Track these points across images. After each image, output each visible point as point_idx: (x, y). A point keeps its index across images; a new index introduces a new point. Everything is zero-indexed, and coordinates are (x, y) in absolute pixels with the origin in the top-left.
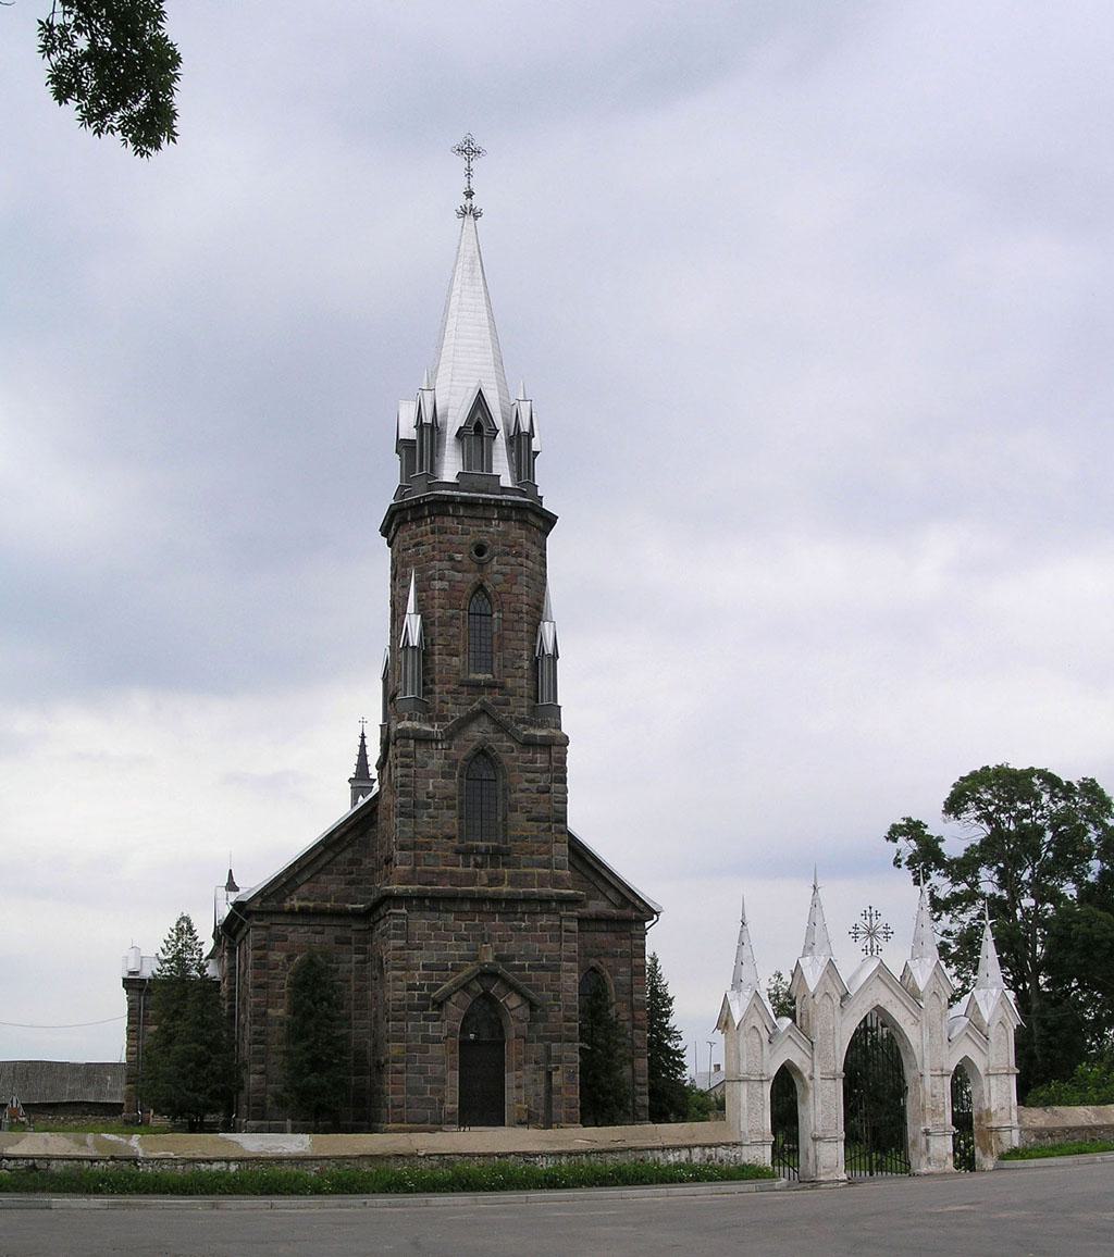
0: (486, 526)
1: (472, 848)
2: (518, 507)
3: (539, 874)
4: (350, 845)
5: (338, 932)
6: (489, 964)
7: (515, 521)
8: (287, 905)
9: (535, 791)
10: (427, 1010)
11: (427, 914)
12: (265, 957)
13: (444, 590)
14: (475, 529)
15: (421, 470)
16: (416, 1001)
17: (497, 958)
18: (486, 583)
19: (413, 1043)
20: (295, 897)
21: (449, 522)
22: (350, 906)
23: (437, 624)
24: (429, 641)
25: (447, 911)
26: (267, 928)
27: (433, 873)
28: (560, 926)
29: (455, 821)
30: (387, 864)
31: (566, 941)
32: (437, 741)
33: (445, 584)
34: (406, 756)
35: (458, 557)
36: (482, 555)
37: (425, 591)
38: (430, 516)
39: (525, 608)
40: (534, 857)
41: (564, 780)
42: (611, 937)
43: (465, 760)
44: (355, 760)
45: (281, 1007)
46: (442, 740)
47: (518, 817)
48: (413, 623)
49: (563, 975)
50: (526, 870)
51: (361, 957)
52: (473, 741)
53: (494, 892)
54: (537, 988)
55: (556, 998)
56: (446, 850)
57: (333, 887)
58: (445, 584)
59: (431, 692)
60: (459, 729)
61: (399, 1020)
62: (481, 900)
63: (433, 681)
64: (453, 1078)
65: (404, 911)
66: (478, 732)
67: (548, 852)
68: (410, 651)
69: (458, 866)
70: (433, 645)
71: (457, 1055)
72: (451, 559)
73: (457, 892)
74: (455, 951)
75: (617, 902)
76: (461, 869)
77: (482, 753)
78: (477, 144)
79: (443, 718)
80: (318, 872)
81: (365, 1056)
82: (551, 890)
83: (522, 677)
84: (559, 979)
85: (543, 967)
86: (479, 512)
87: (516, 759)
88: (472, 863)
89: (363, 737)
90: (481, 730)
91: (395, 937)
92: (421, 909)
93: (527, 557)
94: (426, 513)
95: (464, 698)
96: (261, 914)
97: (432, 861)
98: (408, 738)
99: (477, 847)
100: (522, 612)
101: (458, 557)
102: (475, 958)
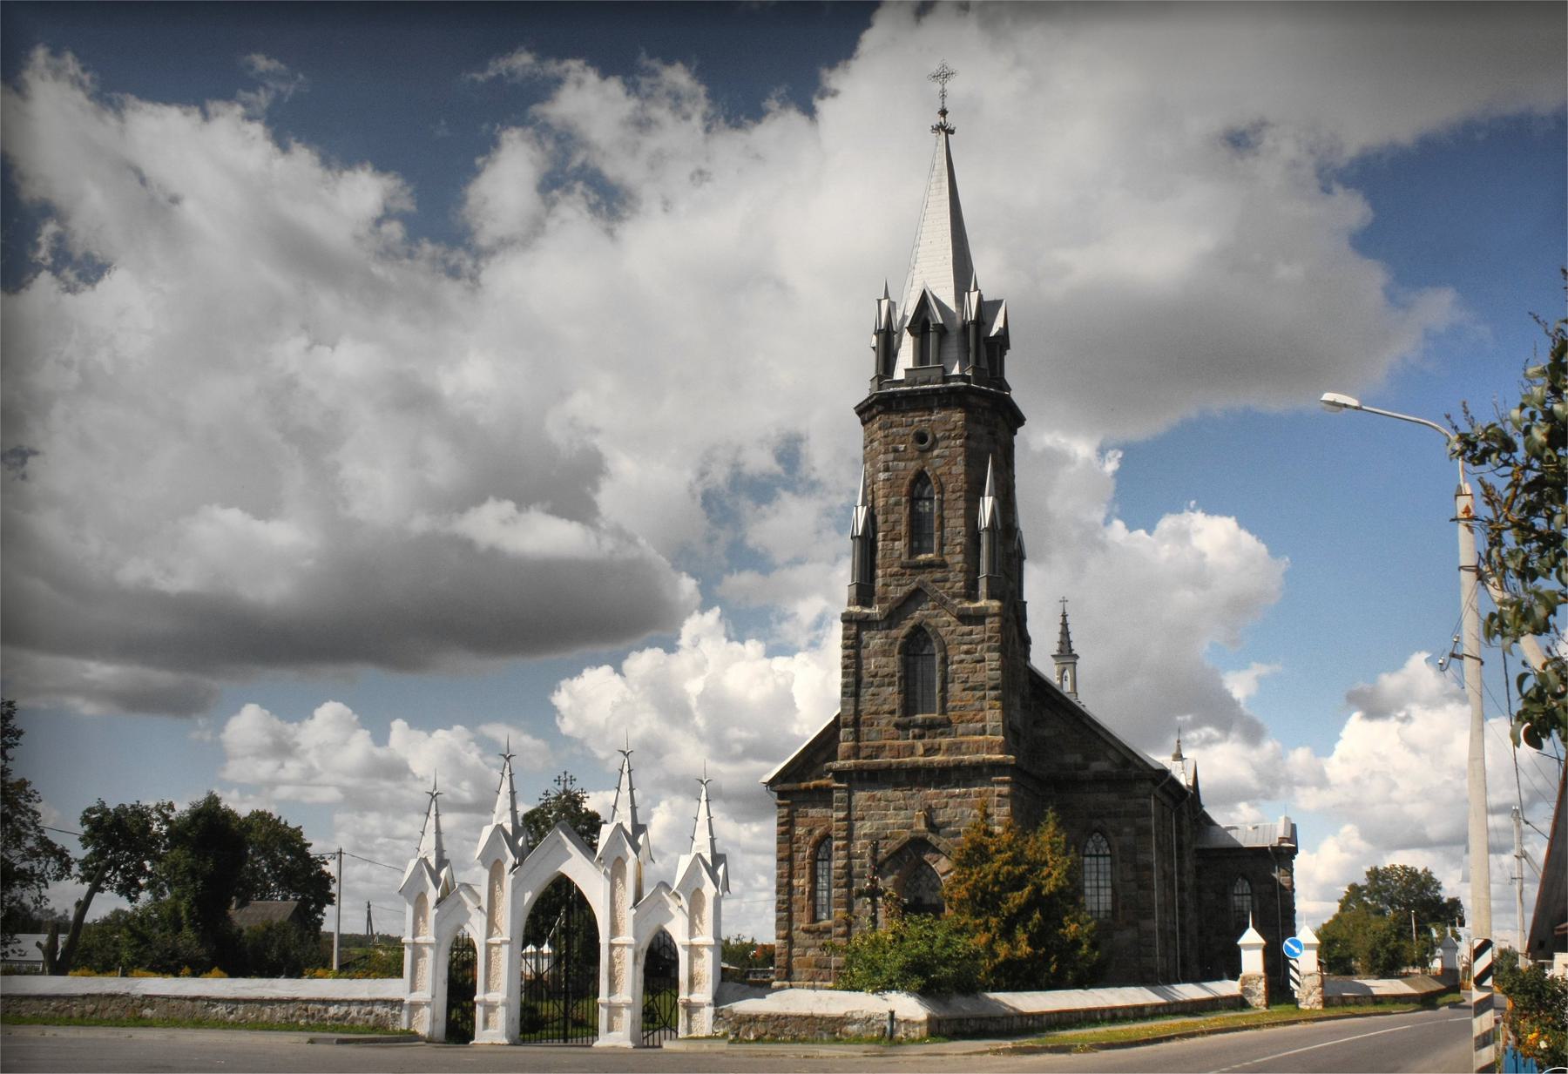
0: (929, 415)
6: (918, 831)
14: (917, 419)
21: (895, 418)
31: (998, 806)
35: (902, 447)
36: (926, 440)
43: (905, 637)
44: (1058, 637)
45: (803, 877)
47: (955, 688)
50: (962, 739)
69: (897, 739)
72: (896, 450)
73: (932, 763)
74: (894, 819)
88: (911, 735)
89: (1064, 616)
102: (910, 827)
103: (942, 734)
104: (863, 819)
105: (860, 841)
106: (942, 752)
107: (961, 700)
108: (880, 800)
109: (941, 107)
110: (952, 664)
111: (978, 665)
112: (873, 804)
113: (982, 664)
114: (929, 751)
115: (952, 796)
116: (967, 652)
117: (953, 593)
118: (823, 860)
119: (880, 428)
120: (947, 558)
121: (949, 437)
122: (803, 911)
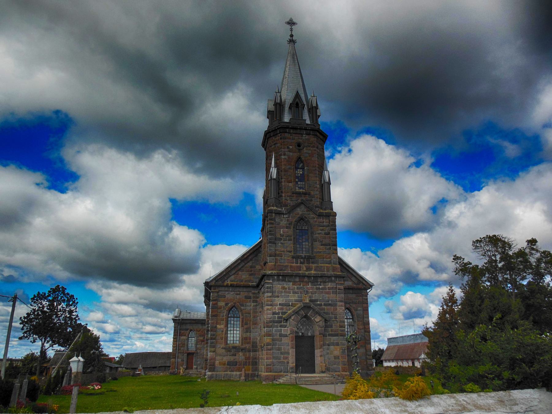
0: (301, 137)
1: (299, 256)
2: (312, 130)
3: (327, 267)
4: (251, 260)
5: (246, 294)
6: (307, 303)
7: (312, 135)
8: (225, 284)
9: (324, 234)
10: (281, 322)
11: (281, 283)
12: (217, 304)
13: (285, 159)
14: (297, 137)
15: (276, 118)
16: (276, 319)
17: (310, 301)
18: (302, 157)
19: (275, 337)
20: (229, 280)
21: (287, 135)
22: (251, 284)
23: (283, 171)
24: (280, 177)
25: (289, 281)
26: (218, 292)
27: (283, 266)
28: (336, 288)
29: (292, 245)
30: (265, 266)
31: (338, 294)
32: (284, 214)
33: (286, 157)
34: (271, 220)
35: (291, 147)
37: (278, 160)
38: (280, 133)
39: (317, 165)
40: (325, 260)
41: (335, 230)
42: (354, 296)
45: (222, 325)
46: (286, 214)
48: (274, 171)
49: (338, 308)
50: (321, 265)
51: (255, 304)
52: (298, 214)
53: (309, 273)
54: (327, 313)
55: (336, 318)
56: (289, 257)
57: (244, 277)
58: (286, 157)
59: (281, 196)
60: (293, 210)
61: (269, 327)
62: (304, 276)
63: (282, 192)
64: (292, 352)
65: (271, 281)
66: (300, 211)
67: (330, 258)
68: (273, 181)
69: (293, 263)
70: (282, 179)
71: (294, 342)
72: (288, 148)
74: (293, 298)
75: (356, 282)
76: (294, 264)
77: (302, 219)
78: (294, 21)
79: (286, 206)
80: (239, 270)
81: (257, 344)
82: (331, 273)
83: (317, 191)
84: (336, 309)
85: (330, 305)
86: (298, 131)
87: (316, 221)
88: (299, 262)
90: (301, 210)
91: (268, 292)
92: (278, 280)
93: (317, 148)
94: (278, 132)
95: (294, 199)
96: (216, 286)
97: (282, 261)
98: (272, 213)
99: (301, 256)
100: (316, 167)
101: (291, 147)
102: (301, 301)
103: (313, 263)
104: (279, 297)
105: (277, 307)
106: (313, 270)
107: (320, 249)
108: (286, 289)
109: (291, 33)
110: (316, 234)
111: (327, 236)
112: (283, 291)
113: (329, 235)
114: (308, 269)
115: (319, 289)
116: (322, 230)
117: (315, 206)
118: (231, 317)
119: (281, 139)
120: (312, 193)
121: (309, 146)
122: (222, 339)
